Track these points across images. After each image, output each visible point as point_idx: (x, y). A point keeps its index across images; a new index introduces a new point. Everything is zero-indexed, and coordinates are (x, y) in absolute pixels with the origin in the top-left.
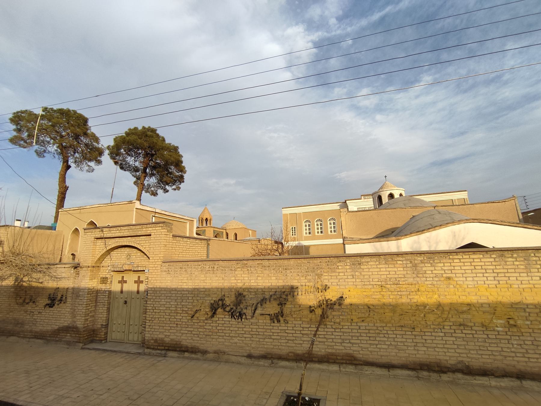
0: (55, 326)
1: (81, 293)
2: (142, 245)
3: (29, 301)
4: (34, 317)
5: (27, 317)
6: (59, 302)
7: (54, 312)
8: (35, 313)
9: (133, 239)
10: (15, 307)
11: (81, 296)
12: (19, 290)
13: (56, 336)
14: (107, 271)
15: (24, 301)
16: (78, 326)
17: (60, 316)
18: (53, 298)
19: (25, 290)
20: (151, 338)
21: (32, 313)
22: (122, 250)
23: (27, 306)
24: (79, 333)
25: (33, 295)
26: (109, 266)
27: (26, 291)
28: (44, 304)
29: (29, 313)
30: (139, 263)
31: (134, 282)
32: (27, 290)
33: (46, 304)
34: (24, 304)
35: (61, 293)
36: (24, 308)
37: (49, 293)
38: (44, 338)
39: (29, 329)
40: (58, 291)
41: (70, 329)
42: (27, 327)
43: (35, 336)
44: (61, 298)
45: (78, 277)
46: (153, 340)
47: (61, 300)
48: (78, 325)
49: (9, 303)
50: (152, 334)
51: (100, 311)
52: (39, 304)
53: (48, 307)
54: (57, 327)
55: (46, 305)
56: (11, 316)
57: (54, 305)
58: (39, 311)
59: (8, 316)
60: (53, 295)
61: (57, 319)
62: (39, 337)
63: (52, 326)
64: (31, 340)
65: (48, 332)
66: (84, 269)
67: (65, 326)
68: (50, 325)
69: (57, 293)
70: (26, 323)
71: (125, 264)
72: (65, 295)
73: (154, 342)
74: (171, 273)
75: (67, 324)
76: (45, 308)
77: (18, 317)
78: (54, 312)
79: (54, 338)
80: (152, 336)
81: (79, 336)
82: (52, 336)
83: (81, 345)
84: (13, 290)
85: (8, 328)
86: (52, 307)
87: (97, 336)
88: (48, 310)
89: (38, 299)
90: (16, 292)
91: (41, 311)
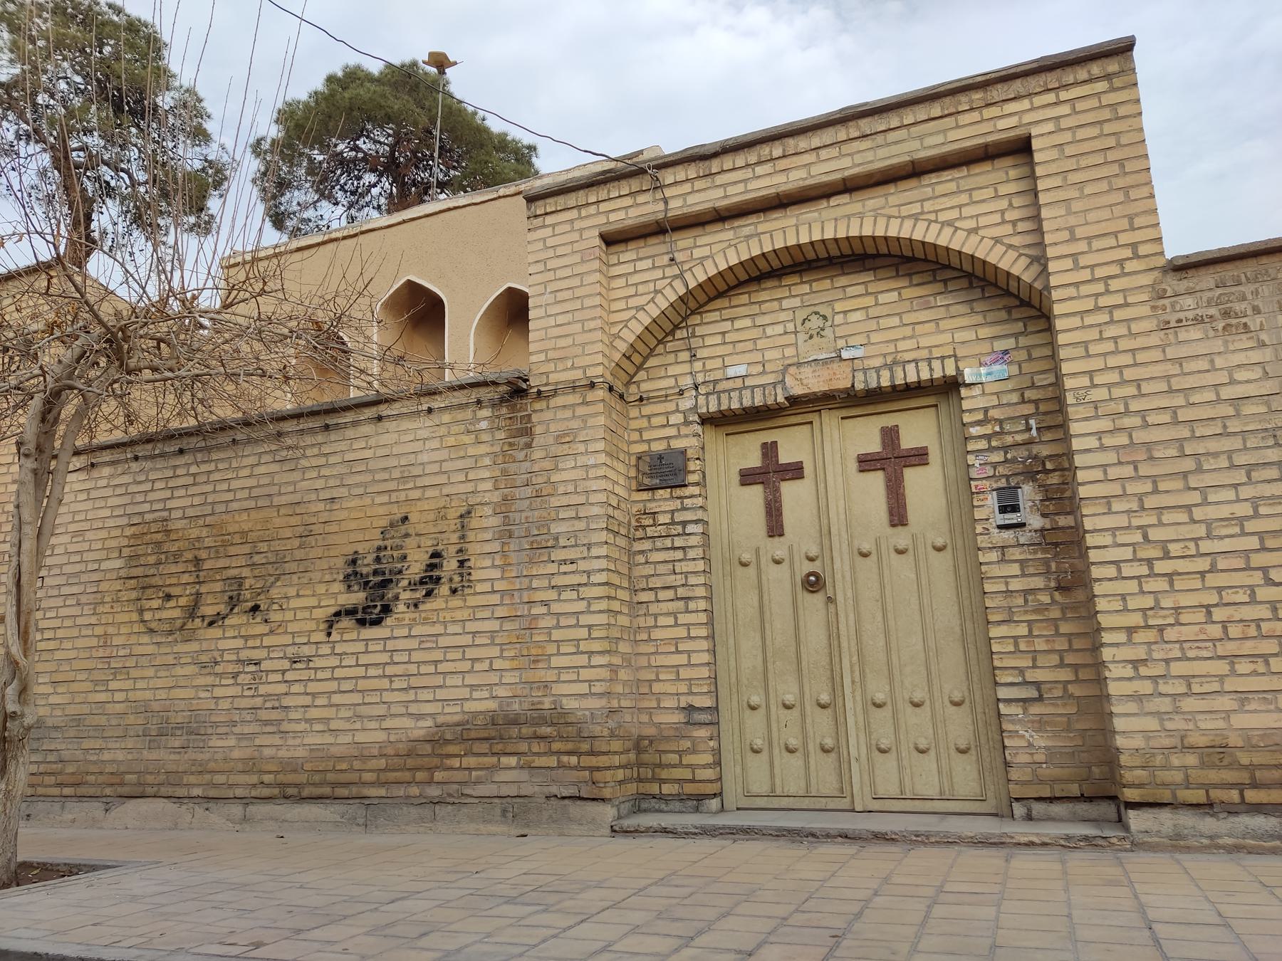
0: (407, 723)
1: (556, 528)
2: (943, 217)
3: (223, 609)
4: (263, 689)
5: (219, 692)
6: (420, 594)
7: (391, 645)
8: (265, 665)
9: (873, 201)
10: (139, 650)
11: (562, 542)
12: (152, 559)
13: (420, 776)
14: (677, 419)
15: (192, 612)
16: (570, 704)
17: (436, 662)
18: (375, 573)
19: (189, 555)
20: (1167, 742)
21: (252, 668)
22: (764, 296)
23: (215, 632)
24: (585, 747)
25: (246, 572)
26: (681, 393)
27: (197, 561)
28: (321, 614)
29: (231, 668)
30: (902, 346)
31: (853, 465)
32: (203, 554)
33: (333, 610)
34: (189, 626)
35: (428, 542)
36: (194, 646)
37: (350, 550)
38: (344, 792)
39: (236, 754)
40: (407, 535)
41: (514, 731)
42: (224, 745)
43: (281, 785)
44: (431, 567)
45: (529, 446)
46: (1188, 748)
47: (429, 581)
48: (564, 701)
49: (99, 631)
50: (1177, 711)
51: (657, 634)
52: (289, 615)
53: (346, 622)
54: (429, 723)
55: (338, 614)
56: (119, 696)
57: (386, 610)
58: (291, 651)
59: (102, 697)
60: (378, 559)
61: (415, 682)
62: (305, 793)
63: (385, 725)
64: (258, 810)
65: (364, 758)
66: (559, 401)
67: (476, 714)
68: (371, 718)
69: (400, 547)
70: (216, 725)
71: (799, 365)
72: (453, 549)
73: (1203, 765)
74: (1254, 323)
75: (492, 705)
76: (329, 634)
77: (162, 694)
78: (391, 645)
79: (414, 790)
80: (1177, 724)
81: (588, 761)
82: (392, 776)
83: (607, 813)
84: (118, 563)
85: (106, 756)
86: (377, 622)
87: (664, 774)
88: (351, 637)
89: (274, 593)
90: (138, 572)
91: (307, 650)
